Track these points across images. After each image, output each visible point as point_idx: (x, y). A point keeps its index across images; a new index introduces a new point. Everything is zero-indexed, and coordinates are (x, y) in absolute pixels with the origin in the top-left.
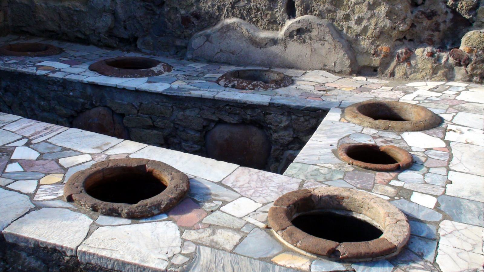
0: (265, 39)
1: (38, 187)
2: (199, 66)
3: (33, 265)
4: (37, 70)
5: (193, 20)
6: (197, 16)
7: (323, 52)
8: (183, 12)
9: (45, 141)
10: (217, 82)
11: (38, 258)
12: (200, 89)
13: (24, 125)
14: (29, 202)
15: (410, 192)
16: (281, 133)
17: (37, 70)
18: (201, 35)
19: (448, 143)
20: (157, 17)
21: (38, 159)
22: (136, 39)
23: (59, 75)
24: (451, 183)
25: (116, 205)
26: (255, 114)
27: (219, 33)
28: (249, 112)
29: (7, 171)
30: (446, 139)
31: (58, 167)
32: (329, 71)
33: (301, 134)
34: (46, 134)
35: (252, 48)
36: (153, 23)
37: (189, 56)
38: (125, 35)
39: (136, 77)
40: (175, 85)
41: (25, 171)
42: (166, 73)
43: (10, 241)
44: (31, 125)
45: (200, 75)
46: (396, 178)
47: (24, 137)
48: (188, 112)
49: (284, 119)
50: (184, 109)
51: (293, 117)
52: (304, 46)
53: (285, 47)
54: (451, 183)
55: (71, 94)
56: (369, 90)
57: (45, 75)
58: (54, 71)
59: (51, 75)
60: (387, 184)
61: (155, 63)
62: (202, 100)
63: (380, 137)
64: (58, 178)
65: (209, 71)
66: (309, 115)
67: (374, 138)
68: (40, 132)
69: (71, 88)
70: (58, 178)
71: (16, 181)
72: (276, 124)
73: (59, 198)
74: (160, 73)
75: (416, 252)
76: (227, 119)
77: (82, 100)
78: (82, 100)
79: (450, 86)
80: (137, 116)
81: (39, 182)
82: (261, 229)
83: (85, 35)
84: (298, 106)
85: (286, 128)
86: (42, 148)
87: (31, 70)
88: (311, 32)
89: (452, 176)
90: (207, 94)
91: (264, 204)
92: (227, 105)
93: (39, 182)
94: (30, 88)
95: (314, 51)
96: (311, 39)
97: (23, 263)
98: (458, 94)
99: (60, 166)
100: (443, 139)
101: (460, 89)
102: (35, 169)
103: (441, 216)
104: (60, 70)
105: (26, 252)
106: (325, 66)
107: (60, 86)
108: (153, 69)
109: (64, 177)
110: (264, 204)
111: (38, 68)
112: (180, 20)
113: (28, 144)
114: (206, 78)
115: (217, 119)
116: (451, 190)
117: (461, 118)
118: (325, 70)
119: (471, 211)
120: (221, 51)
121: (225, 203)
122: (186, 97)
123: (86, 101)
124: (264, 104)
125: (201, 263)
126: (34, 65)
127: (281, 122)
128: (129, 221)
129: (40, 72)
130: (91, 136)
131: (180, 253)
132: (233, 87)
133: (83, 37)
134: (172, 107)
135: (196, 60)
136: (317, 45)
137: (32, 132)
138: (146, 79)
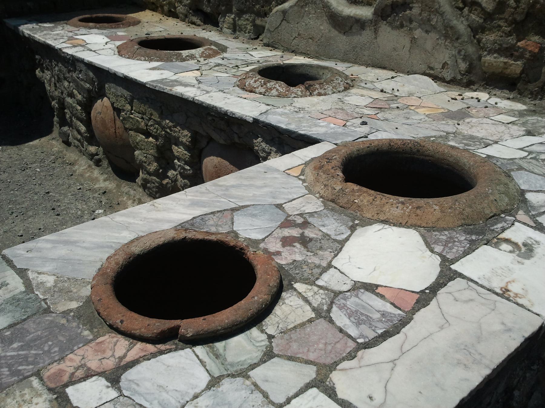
0: (349, 17)
7: (429, 45)
35: (334, 33)
53: (376, 31)
57: (60, 49)
78: (88, 85)
80: (132, 114)
88: (411, 9)
95: (413, 40)
106: (432, 68)
118: (429, 75)
120: (299, 35)
134: (161, 107)
136: (418, 33)
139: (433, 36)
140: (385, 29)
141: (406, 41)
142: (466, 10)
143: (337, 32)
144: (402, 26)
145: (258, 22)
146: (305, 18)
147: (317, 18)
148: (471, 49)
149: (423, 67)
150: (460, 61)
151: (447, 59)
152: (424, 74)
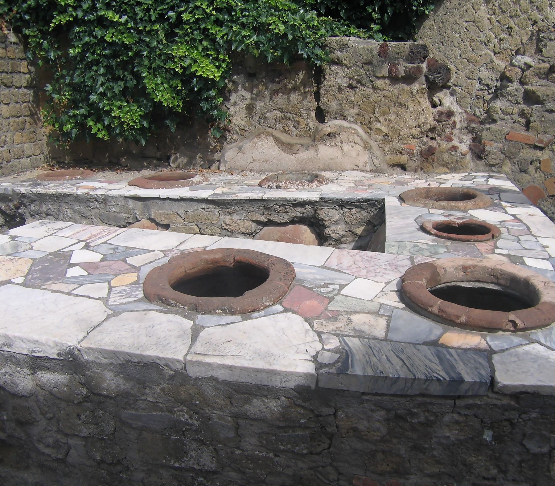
1: (110, 288)
7: (354, 154)
10: (260, 185)
12: (244, 191)
13: (78, 230)
14: (104, 308)
21: (101, 261)
23: (100, 192)
26: (305, 211)
28: (299, 209)
29: (68, 275)
32: (361, 171)
34: (104, 236)
41: (89, 274)
43: (91, 358)
44: (85, 230)
47: (80, 241)
52: (336, 149)
53: (317, 151)
55: (113, 209)
57: (86, 194)
58: (95, 189)
62: (251, 201)
64: (132, 277)
67: (445, 216)
68: (96, 235)
70: (132, 277)
71: (81, 285)
72: (328, 218)
73: (139, 300)
76: (276, 218)
78: (125, 215)
81: (109, 283)
84: (349, 199)
86: (104, 249)
91: (387, 284)
93: (109, 283)
99: (130, 265)
104: (100, 188)
108: (191, 179)
109: (139, 276)
111: (78, 188)
113: (87, 247)
114: (246, 184)
115: (266, 220)
120: (254, 160)
121: (342, 287)
123: (129, 216)
124: (315, 199)
129: (80, 192)
130: (156, 234)
132: (278, 187)
136: (346, 147)
137: (89, 235)
138: (188, 188)
143: (286, 155)
150: (375, 160)
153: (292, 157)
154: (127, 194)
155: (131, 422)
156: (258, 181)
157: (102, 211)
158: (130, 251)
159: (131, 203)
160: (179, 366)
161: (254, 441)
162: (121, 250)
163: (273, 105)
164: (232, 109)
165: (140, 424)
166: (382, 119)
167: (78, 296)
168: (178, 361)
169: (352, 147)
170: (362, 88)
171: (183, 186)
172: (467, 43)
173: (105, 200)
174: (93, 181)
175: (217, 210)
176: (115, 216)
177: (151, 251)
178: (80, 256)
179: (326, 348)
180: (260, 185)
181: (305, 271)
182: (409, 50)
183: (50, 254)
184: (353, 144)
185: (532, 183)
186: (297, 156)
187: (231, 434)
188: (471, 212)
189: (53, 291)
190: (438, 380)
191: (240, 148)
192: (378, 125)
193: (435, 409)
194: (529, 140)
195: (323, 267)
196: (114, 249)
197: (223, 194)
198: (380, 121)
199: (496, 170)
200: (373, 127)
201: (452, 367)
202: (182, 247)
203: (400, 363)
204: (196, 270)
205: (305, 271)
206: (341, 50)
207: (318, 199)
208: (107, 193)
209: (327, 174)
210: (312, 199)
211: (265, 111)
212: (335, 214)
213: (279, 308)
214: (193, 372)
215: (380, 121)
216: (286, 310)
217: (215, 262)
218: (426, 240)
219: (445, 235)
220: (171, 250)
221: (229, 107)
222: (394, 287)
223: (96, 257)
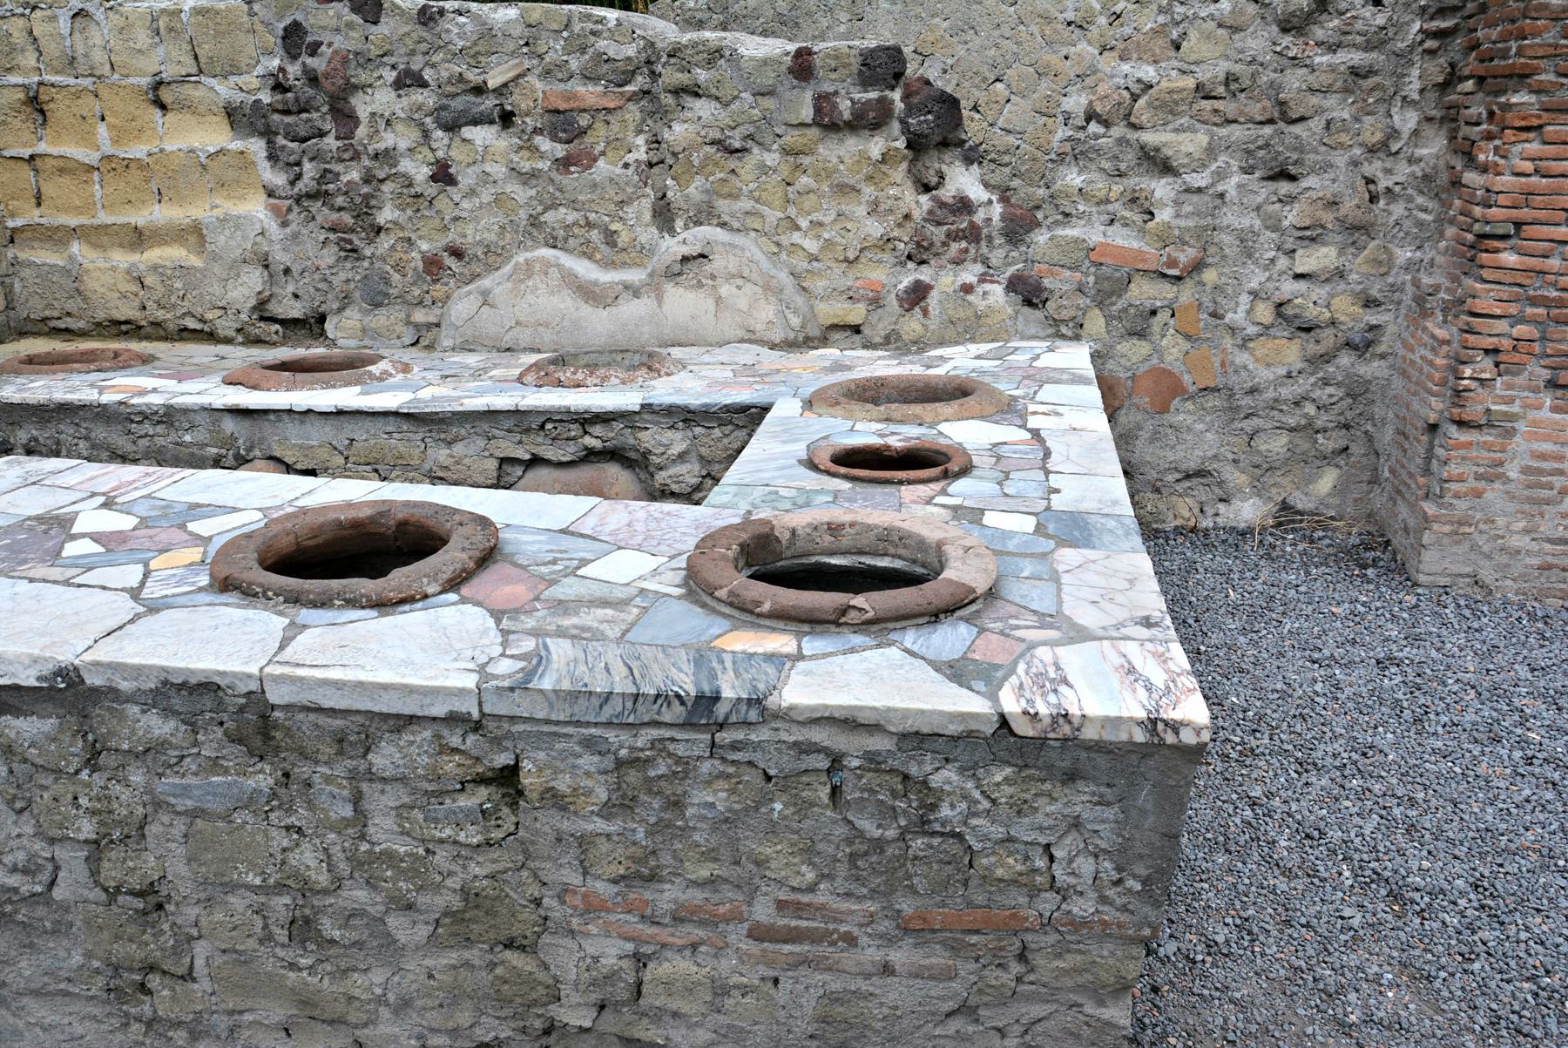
1: (146, 575)
2: (472, 360)
3: (157, 732)
4: (100, 393)
5: (450, 261)
6: (457, 253)
7: (743, 303)
8: (425, 246)
9: (148, 496)
10: (520, 380)
11: (168, 712)
12: (482, 393)
13: (94, 473)
15: (982, 511)
16: (672, 471)
17: (100, 393)
18: (470, 293)
19: (1036, 433)
20: (366, 264)
22: (322, 319)
23: (156, 400)
24: (1057, 491)
25: (335, 584)
26: (611, 435)
27: (509, 285)
28: (597, 430)
29: (64, 554)
30: (1029, 426)
31: (186, 537)
33: (717, 467)
35: (586, 310)
36: (358, 278)
37: (447, 343)
38: (295, 311)
39: (334, 387)
40: (425, 394)
42: (401, 376)
45: (478, 374)
46: (944, 492)
47: (93, 495)
48: (458, 449)
49: (679, 435)
50: (449, 444)
51: (698, 430)
52: (701, 294)
53: (660, 299)
54: (1057, 491)
55: (188, 438)
56: (849, 368)
57: (121, 403)
58: (143, 392)
59: (134, 401)
60: (929, 502)
61: (373, 361)
62: (491, 415)
63: (893, 434)
65: (495, 366)
66: (731, 422)
67: (882, 436)
68: (131, 483)
69: (187, 425)
71: (90, 569)
72: (661, 449)
73: (201, 589)
74: (385, 375)
75: (1018, 600)
76: (550, 453)
77: (215, 450)
78: (215, 450)
79: (1017, 349)
81: (146, 565)
82: (679, 598)
83: (202, 321)
84: (706, 405)
85: (682, 457)
86: (143, 509)
87: (88, 395)
89: (1054, 481)
90: (502, 402)
91: (672, 558)
92: (549, 420)
93: (146, 565)
94: (86, 438)
95: (719, 300)
96: (713, 277)
97: (133, 732)
98: (1037, 357)
99: (191, 534)
100: (1024, 426)
101: (1038, 351)
102: (131, 544)
103: (1052, 544)
104: (155, 390)
105: (137, 703)
107: (159, 422)
109: (205, 552)
110: (672, 558)
112: (420, 265)
113: (108, 504)
115: (528, 457)
116: (1057, 502)
117: (1048, 393)
118: (751, 341)
119: (1111, 531)
121: (584, 562)
122: (454, 413)
123: (223, 451)
124: (630, 408)
125: (555, 666)
126: (92, 386)
127: (668, 447)
128: (374, 613)
130: (254, 480)
131: (503, 655)
133: (198, 326)
135: (466, 347)
136: (725, 290)
138: (358, 389)
139: (749, 288)
140: (672, 292)
141: (710, 304)
142: (784, 256)
143: (590, 309)
144: (700, 285)
145: (420, 316)
146: (528, 296)
147: (552, 293)
148: (800, 300)
149: (741, 333)
151: (771, 316)
152: (742, 341)
153: (605, 313)
154: (219, 403)
155: (172, 800)
156: (517, 372)
157: (160, 441)
158: (196, 510)
159: (229, 425)
160: (254, 686)
161: (389, 823)
162: (179, 508)
163: (558, 194)
164: (465, 204)
165: (190, 803)
166: (804, 223)
167: (80, 586)
168: (250, 676)
169: (739, 287)
170: (756, 150)
171: (348, 384)
172: (1035, 29)
173: (169, 416)
174: (139, 374)
175: (421, 435)
176: (193, 454)
177: (235, 510)
178: (92, 519)
179: (508, 652)
180: (520, 380)
181: (525, 538)
182: (860, 59)
183: (29, 518)
184: (740, 282)
185: (1155, 361)
186: (613, 310)
187: (347, 811)
188: (944, 427)
189: (31, 580)
190: (678, 696)
191: (485, 294)
192: (796, 237)
193: (680, 750)
194: (1144, 261)
195: (563, 531)
196: (166, 507)
197: (434, 399)
198: (798, 228)
199: (1070, 334)
200: (785, 240)
201: (713, 676)
202: (300, 503)
203: (625, 671)
204: (320, 540)
205: (525, 538)
206: (710, 63)
207: (637, 408)
208: (172, 401)
209: (677, 352)
210: (624, 408)
211: (540, 209)
212: (677, 441)
213: (452, 597)
214: (275, 696)
215: (798, 228)
216: (464, 601)
217: (356, 525)
218: (812, 480)
219: (843, 470)
220: (281, 507)
221: (457, 198)
222: (682, 562)
223: (125, 523)
